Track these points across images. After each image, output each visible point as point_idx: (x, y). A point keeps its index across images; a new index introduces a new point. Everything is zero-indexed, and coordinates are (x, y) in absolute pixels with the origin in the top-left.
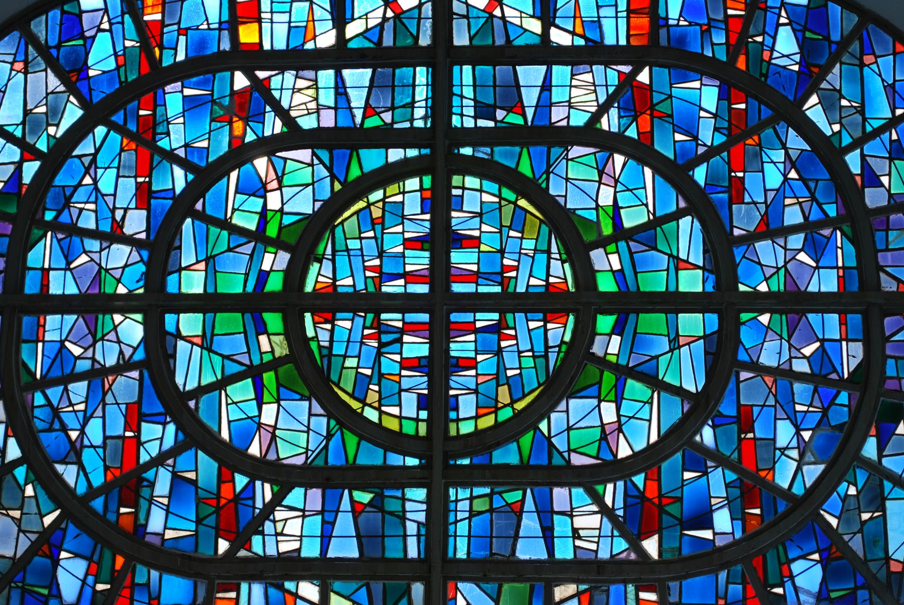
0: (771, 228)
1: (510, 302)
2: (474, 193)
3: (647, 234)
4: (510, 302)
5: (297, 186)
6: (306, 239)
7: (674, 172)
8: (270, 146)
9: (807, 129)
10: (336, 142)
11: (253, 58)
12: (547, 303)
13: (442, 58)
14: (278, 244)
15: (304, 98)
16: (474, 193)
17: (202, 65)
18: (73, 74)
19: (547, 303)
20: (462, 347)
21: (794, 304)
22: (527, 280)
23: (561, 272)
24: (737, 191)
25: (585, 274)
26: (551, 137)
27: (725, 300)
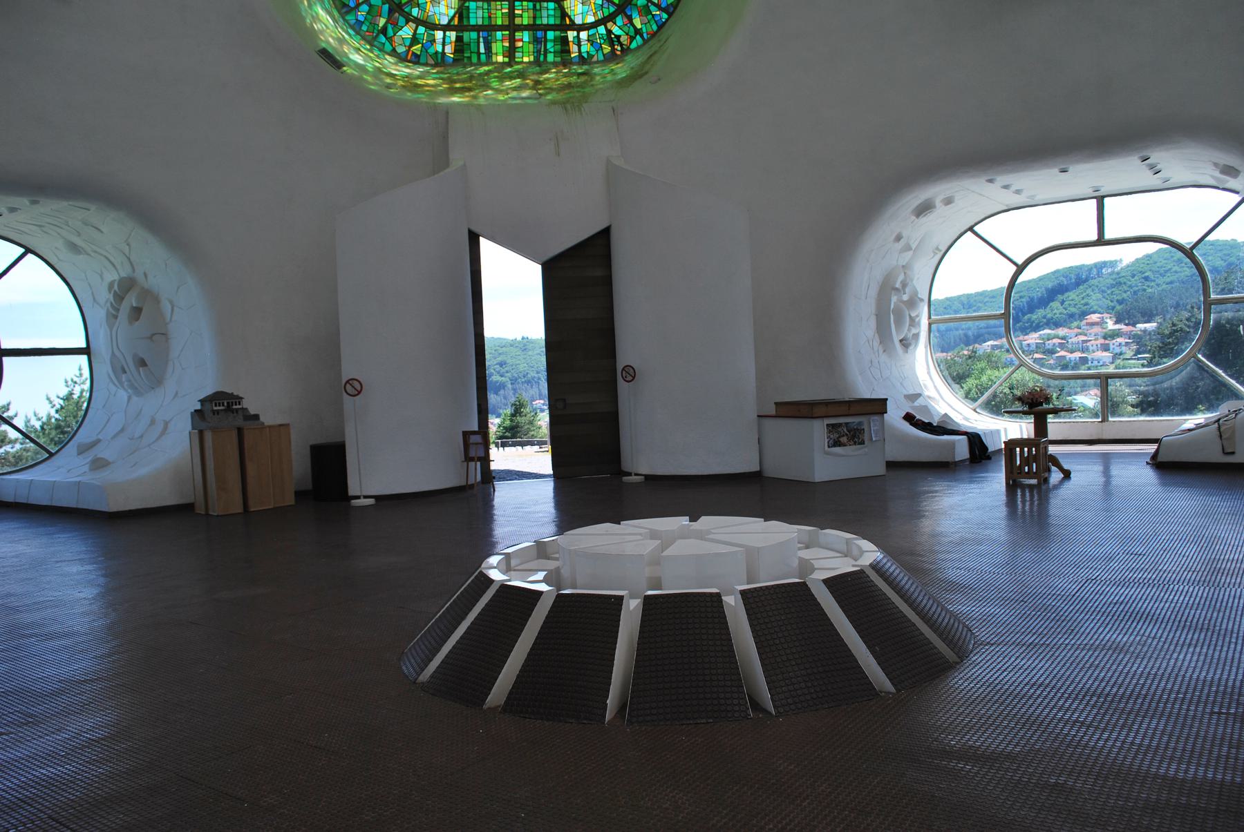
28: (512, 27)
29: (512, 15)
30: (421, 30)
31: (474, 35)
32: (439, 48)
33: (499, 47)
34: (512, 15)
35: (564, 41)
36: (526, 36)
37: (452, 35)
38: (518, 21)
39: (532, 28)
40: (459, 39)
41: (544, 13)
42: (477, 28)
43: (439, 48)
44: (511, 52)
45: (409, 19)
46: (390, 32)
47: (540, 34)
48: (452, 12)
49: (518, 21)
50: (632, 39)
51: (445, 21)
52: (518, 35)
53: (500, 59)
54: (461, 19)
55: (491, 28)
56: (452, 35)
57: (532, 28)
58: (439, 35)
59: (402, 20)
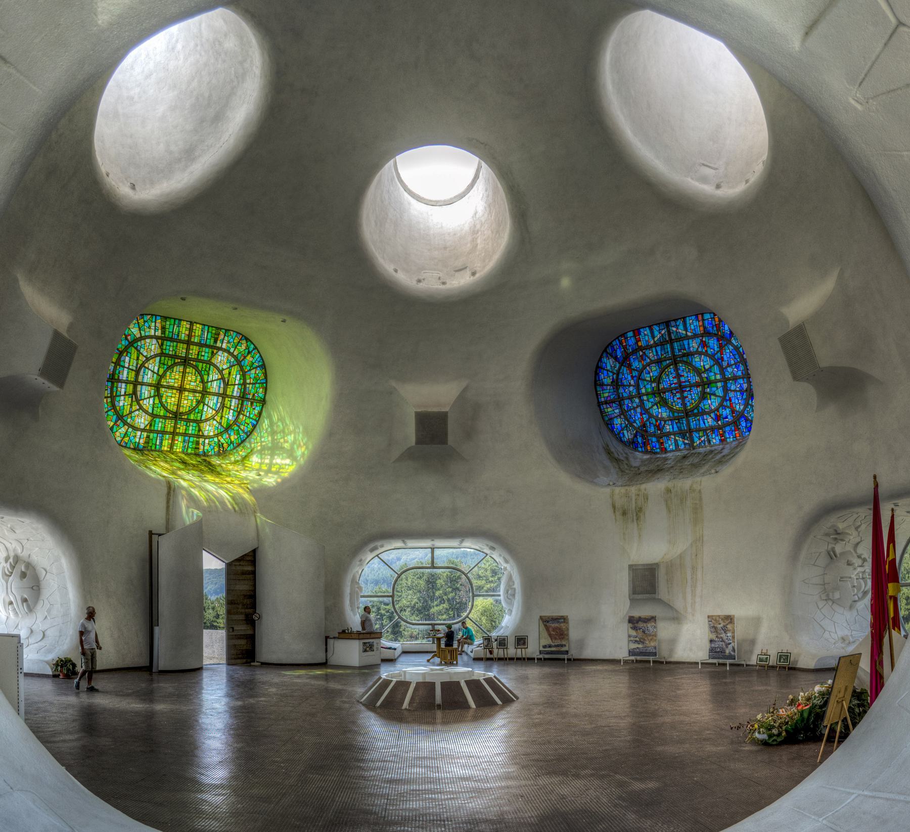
0: (729, 365)
1: (691, 386)
2: (681, 367)
3: (709, 370)
4: (691, 386)
5: (654, 370)
6: (658, 380)
7: (712, 357)
8: (648, 365)
9: (733, 345)
10: (659, 362)
11: (641, 348)
12: (697, 385)
13: (671, 341)
14: (654, 382)
15: (651, 355)
16: (681, 367)
17: (635, 352)
18: (616, 359)
19: (697, 385)
20: (685, 394)
21: (735, 378)
22: (693, 381)
23: (698, 379)
24: (722, 359)
25: (701, 378)
26: (691, 354)
27: (725, 380)
28: (174, 434)
29: (175, 427)
30: (130, 430)
31: (155, 435)
32: (137, 440)
33: (166, 443)
34: (175, 427)
35: (198, 443)
36: (180, 439)
37: (145, 434)
38: (178, 431)
39: (185, 434)
40: (148, 437)
41: (191, 428)
42: (158, 432)
43: (137, 440)
44: (171, 446)
45: (125, 423)
46: (115, 430)
47: (187, 438)
48: (147, 423)
49: (178, 431)
50: (229, 445)
51: (142, 426)
52: (176, 438)
53: (166, 449)
54: (151, 425)
55: (164, 433)
56: (145, 434)
57: (185, 434)
58: (139, 433)
59: (121, 425)
